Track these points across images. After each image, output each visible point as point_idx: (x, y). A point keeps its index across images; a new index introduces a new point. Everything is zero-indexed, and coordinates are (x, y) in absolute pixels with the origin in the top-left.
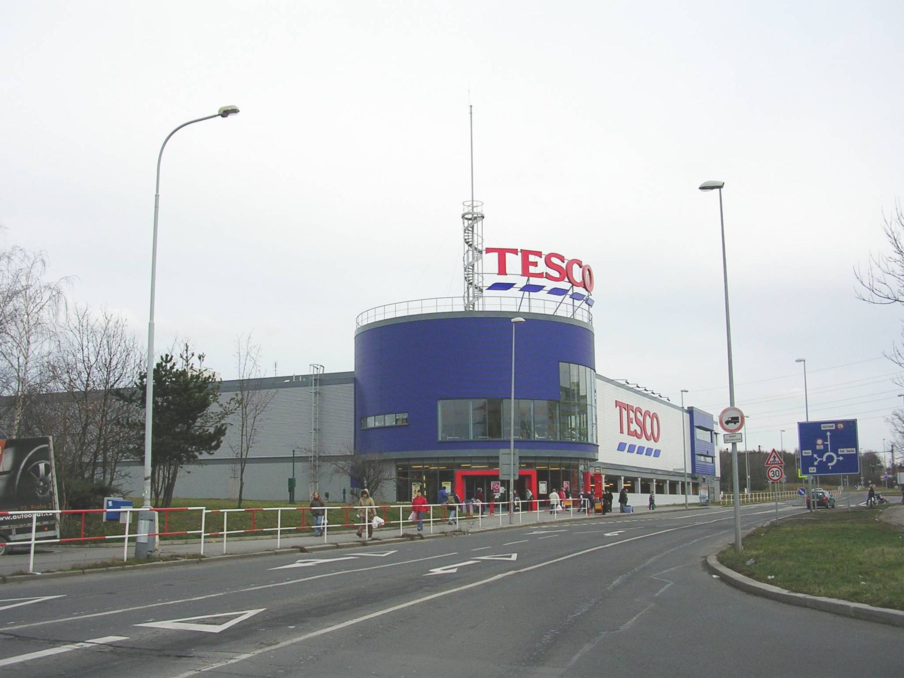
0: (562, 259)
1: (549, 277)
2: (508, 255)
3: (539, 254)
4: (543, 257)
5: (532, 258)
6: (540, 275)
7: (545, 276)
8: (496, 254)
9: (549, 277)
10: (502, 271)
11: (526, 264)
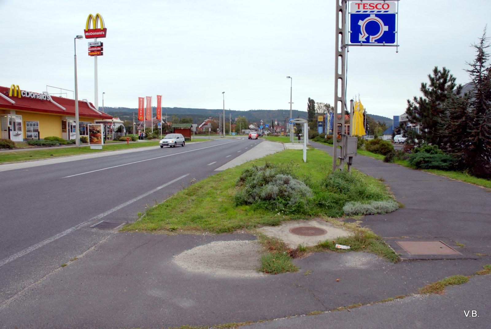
0: (374, 4)
1: (370, 9)
2: (360, 5)
3: (367, 4)
4: (369, 4)
5: (365, 5)
6: (368, 9)
8: (357, 5)
9: (370, 9)
10: (359, 8)
11: (364, 6)
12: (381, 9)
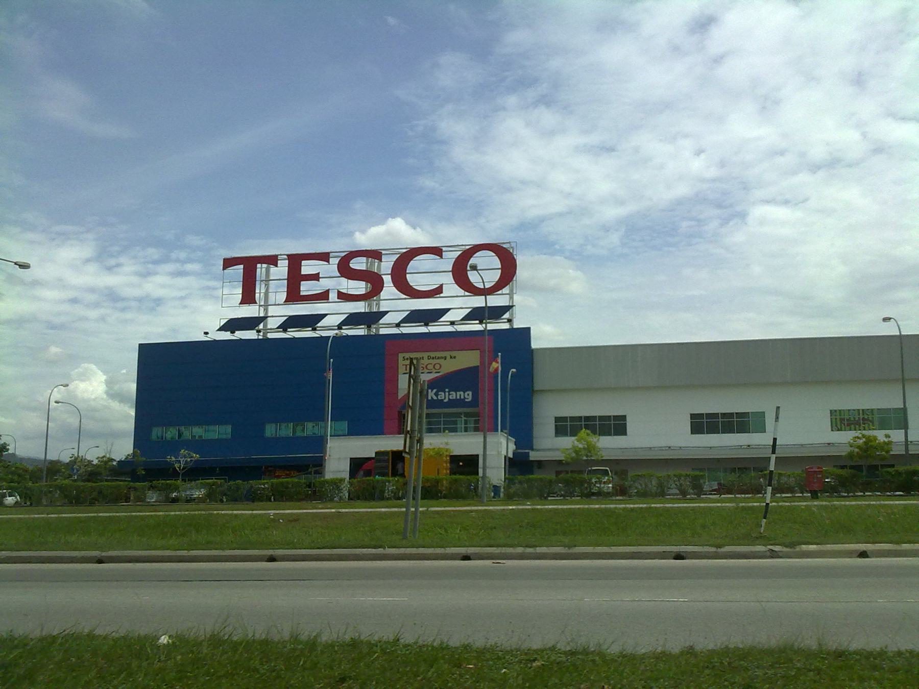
1: (344, 297)
2: (261, 269)
3: (324, 257)
4: (334, 261)
6: (323, 296)
7: (333, 296)
9: (344, 297)
10: (248, 298)
11: (295, 278)
12: (437, 292)
